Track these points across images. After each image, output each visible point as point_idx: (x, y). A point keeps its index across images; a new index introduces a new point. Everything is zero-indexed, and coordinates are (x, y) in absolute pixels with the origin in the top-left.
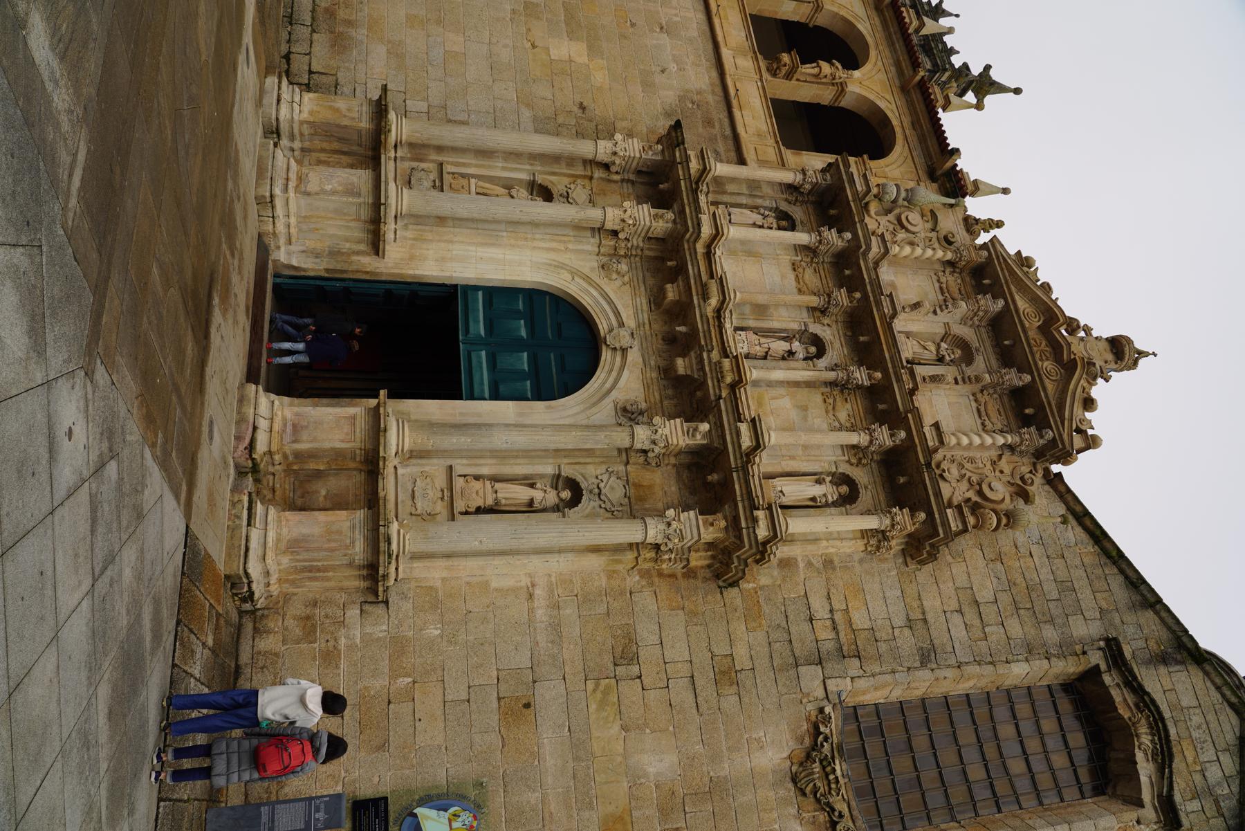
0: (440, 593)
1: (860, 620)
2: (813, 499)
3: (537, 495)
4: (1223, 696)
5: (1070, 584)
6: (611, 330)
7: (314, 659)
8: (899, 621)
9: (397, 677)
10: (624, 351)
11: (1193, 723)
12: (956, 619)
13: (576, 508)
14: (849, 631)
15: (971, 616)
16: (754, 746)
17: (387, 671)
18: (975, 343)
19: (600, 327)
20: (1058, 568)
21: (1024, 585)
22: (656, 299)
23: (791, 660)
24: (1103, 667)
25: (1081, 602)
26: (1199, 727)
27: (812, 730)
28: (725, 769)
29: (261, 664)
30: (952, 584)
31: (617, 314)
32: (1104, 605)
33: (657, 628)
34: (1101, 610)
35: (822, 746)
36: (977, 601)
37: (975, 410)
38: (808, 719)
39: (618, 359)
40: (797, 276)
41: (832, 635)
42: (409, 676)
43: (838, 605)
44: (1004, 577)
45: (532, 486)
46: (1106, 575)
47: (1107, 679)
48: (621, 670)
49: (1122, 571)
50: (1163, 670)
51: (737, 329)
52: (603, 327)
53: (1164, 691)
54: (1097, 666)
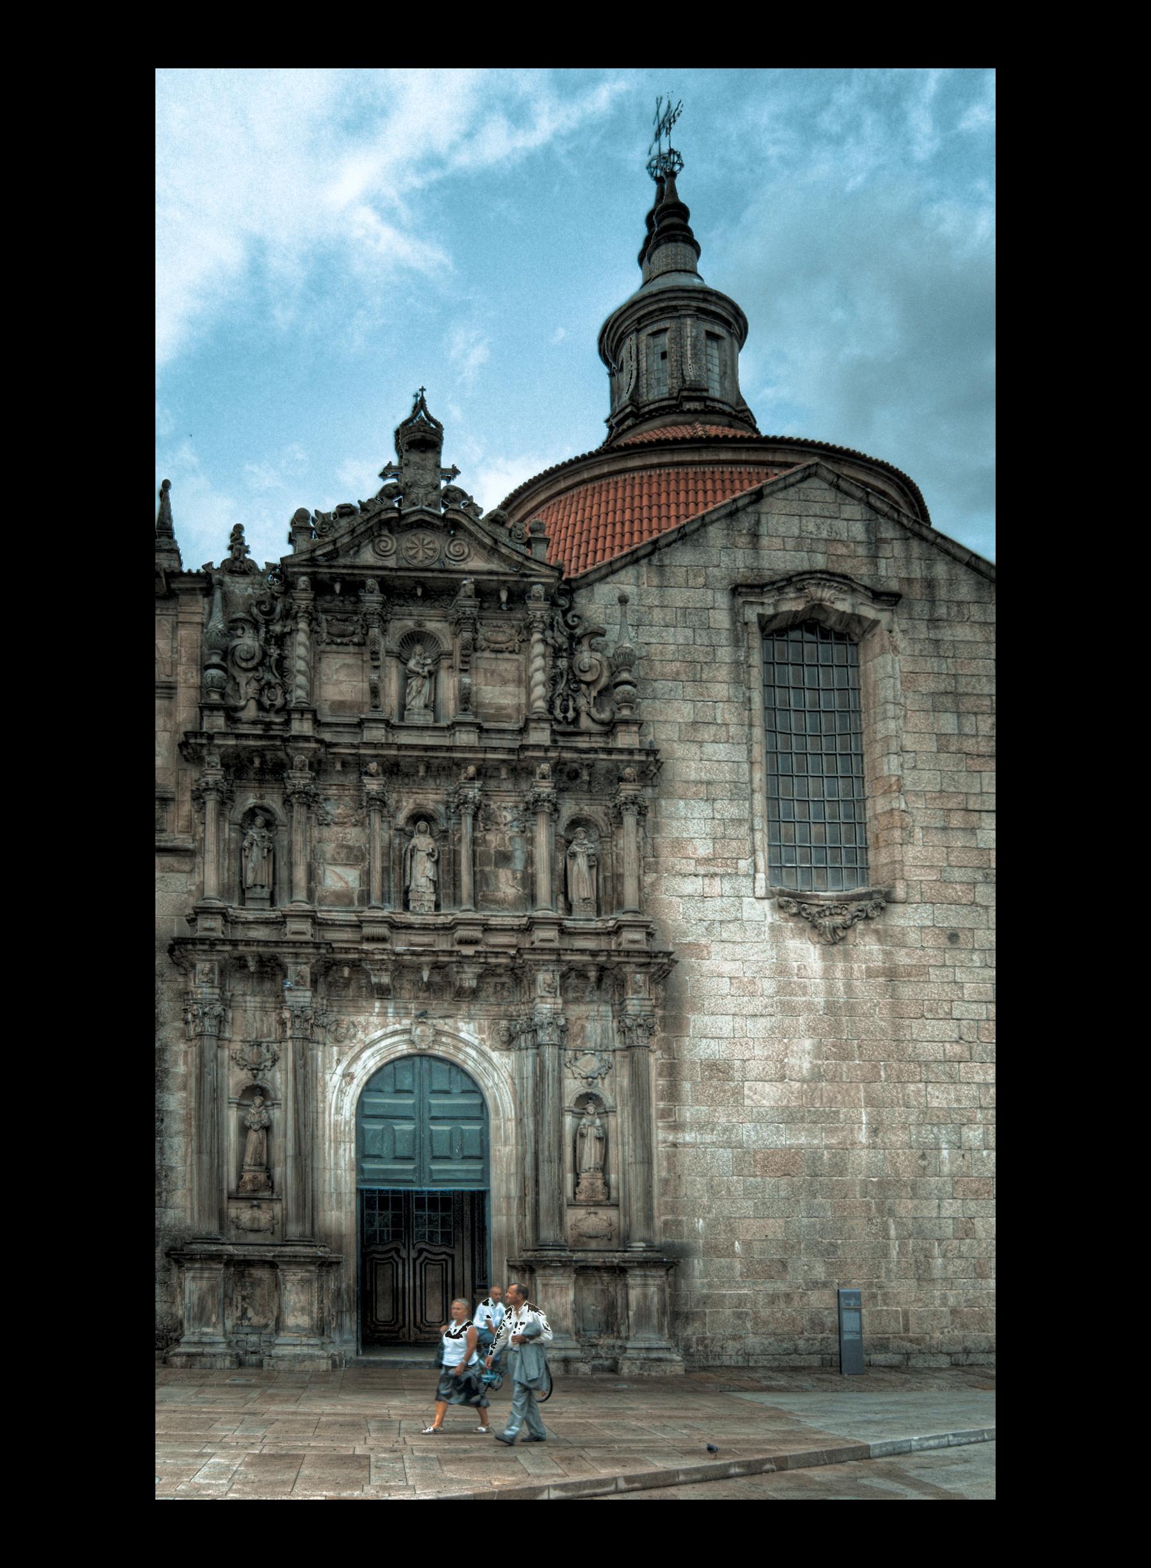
0: (669, 1217)
1: (703, 849)
2: (591, 867)
3: (592, 1132)
4: (793, 485)
5: (679, 611)
6: (412, 1042)
7: (718, 1312)
8: (708, 812)
9: (734, 1252)
10: (439, 1033)
11: (814, 530)
12: (709, 749)
13: (604, 1100)
14: (713, 863)
15: (707, 734)
16: (803, 972)
17: (728, 1260)
18: (410, 624)
19: (405, 1052)
20: (664, 619)
21: (678, 664)
22: (383, 992)
23: (737, 924)
24: (759, 610)
25: (698, 606)
26: (818, 527)
27: (796, 919)
28: (820, 1000)
29: (719, 1350)
30: (675, 745)
31: (395, 1033)
32: (701, 580)
33: (704, 1041)
34: (705, 586)
35: (810, 914)
36: (695, 723)
37: (493, 655)
38: (786, 921)
39: (444, 1039)
40: (336, 824)
41: (718, 879)
42: (733, 1244)
43: (691, 867)
44: (670, 684)
45: (582, 1136)
46: (670, 565)
47: (770, 611)
48: (738, 1076)
49: (668, 545)
50: (764, 541)
51: (406, 906)
52: (404, 1049)
53: (784, 550)
54: (760, 616)
